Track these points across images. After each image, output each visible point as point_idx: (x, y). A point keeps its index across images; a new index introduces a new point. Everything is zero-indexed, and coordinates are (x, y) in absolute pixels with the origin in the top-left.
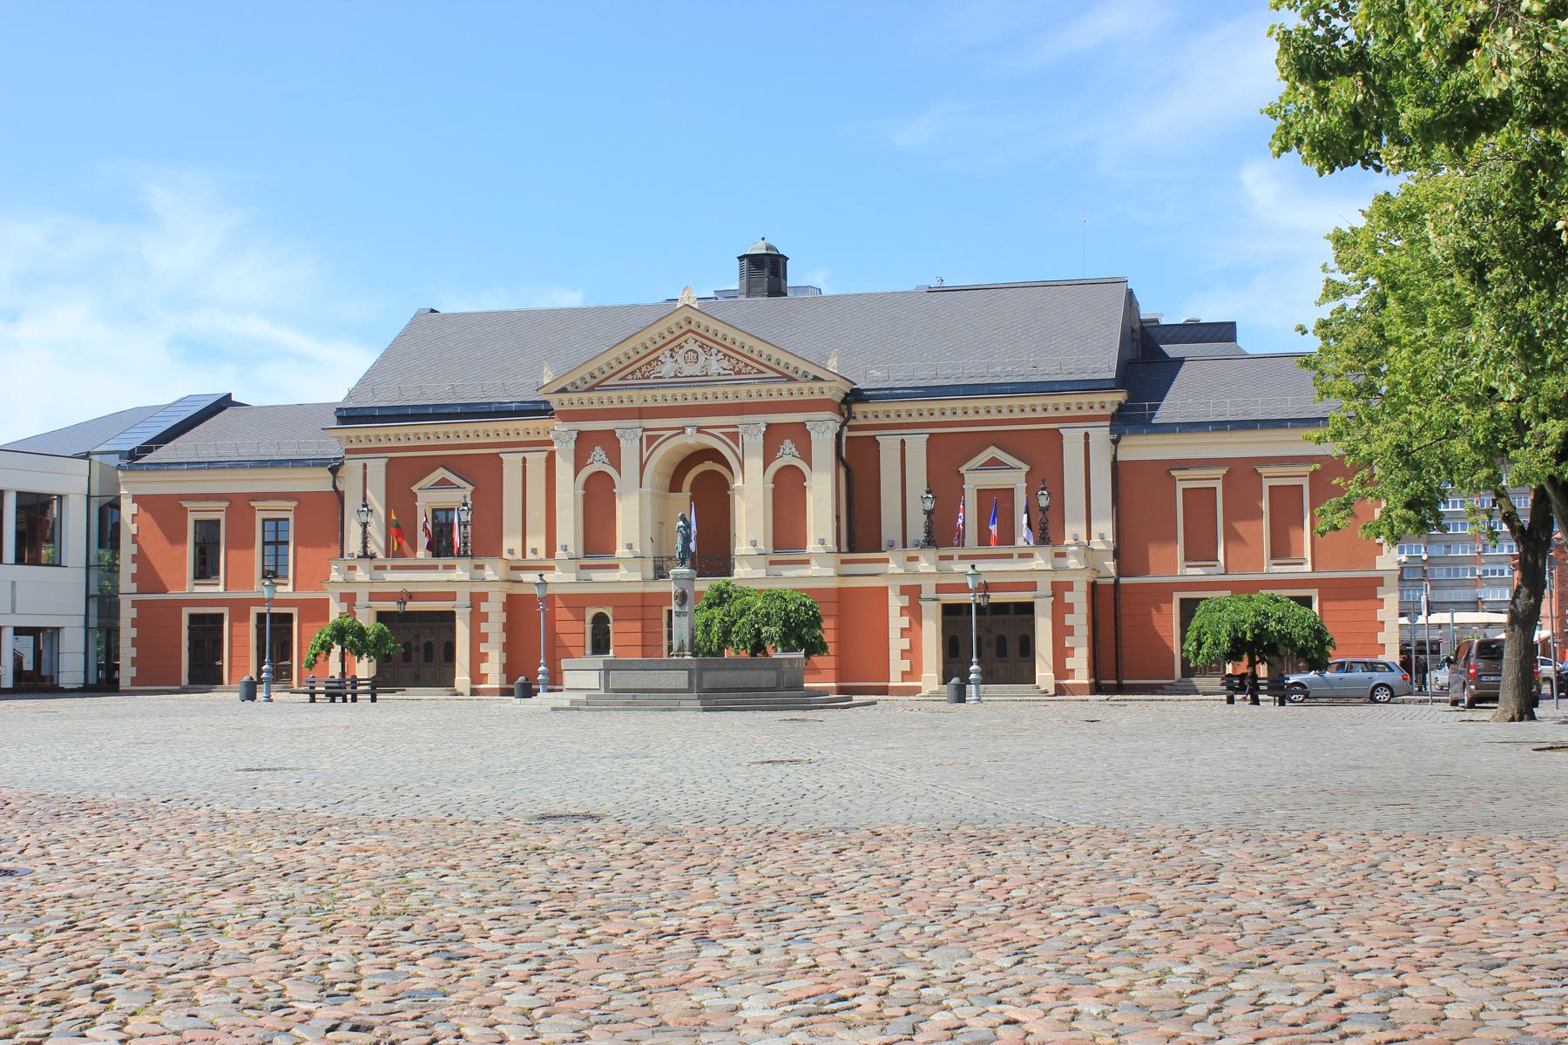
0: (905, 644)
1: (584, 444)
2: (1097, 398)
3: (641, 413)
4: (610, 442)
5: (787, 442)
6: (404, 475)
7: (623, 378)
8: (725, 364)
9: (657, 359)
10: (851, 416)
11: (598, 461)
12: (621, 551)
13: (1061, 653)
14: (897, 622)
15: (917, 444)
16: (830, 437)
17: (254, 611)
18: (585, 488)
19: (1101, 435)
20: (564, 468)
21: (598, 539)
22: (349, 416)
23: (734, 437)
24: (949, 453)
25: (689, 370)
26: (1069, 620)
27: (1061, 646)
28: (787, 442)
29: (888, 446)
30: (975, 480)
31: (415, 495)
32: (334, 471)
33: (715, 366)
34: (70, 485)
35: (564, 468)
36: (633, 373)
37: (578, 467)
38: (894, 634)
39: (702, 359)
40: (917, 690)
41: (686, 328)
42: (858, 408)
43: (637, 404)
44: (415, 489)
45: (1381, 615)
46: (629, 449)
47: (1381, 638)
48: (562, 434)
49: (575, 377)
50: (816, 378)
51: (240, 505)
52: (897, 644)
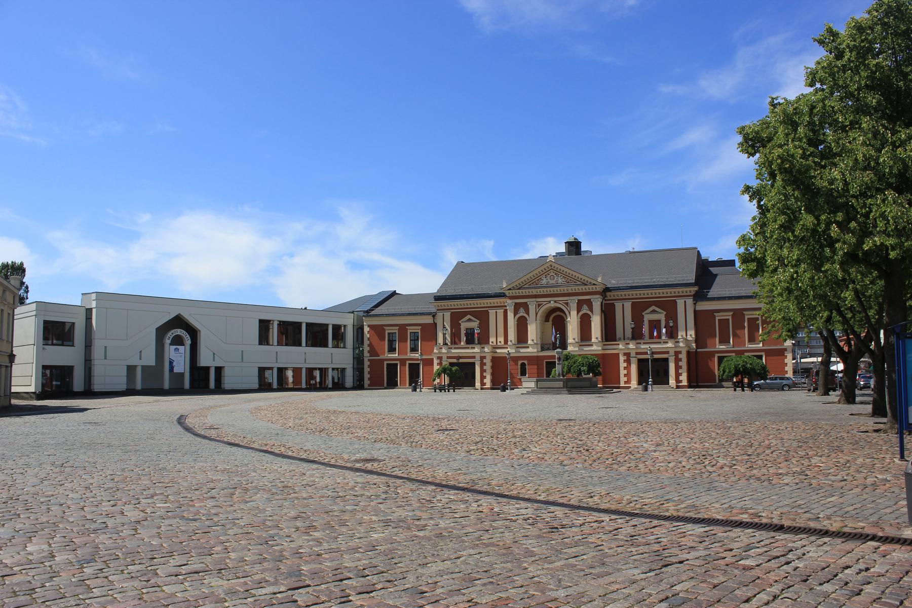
0: (625, 372)
1: (517, 308)
2: (688, 289)
3: (536, 296)
4: (526, 307)
6: (456, 317)
10: (606, 296)
11: (522, 313)
12: (530, 342)
13: (678, 375)
14: (623, 365)
15: (628, 305)
16: (599, 303)
17: (408, 362)
19: (690, 301)
20: (510, 315)
21: (522, 338)
22: (438, 298)
23: (567, 304)
24: (639, 309)
25: (551, 282)
26: (680, 364)
27: (678, 374)
29: (618, 306)
30: (648, 317)
32: (434, 316)
33: (560, 280)
34: (348, 321)
35: (510, 315)
38: (622, 369)
40: (629, 387)
42: (608, 294)
43: (535, 293)
45: (786, 361)
46: (532, 308)
47: (786, 369)
48: (510, 304)
49: (514, 285)
51: (403, 328)
52: (623, 372)
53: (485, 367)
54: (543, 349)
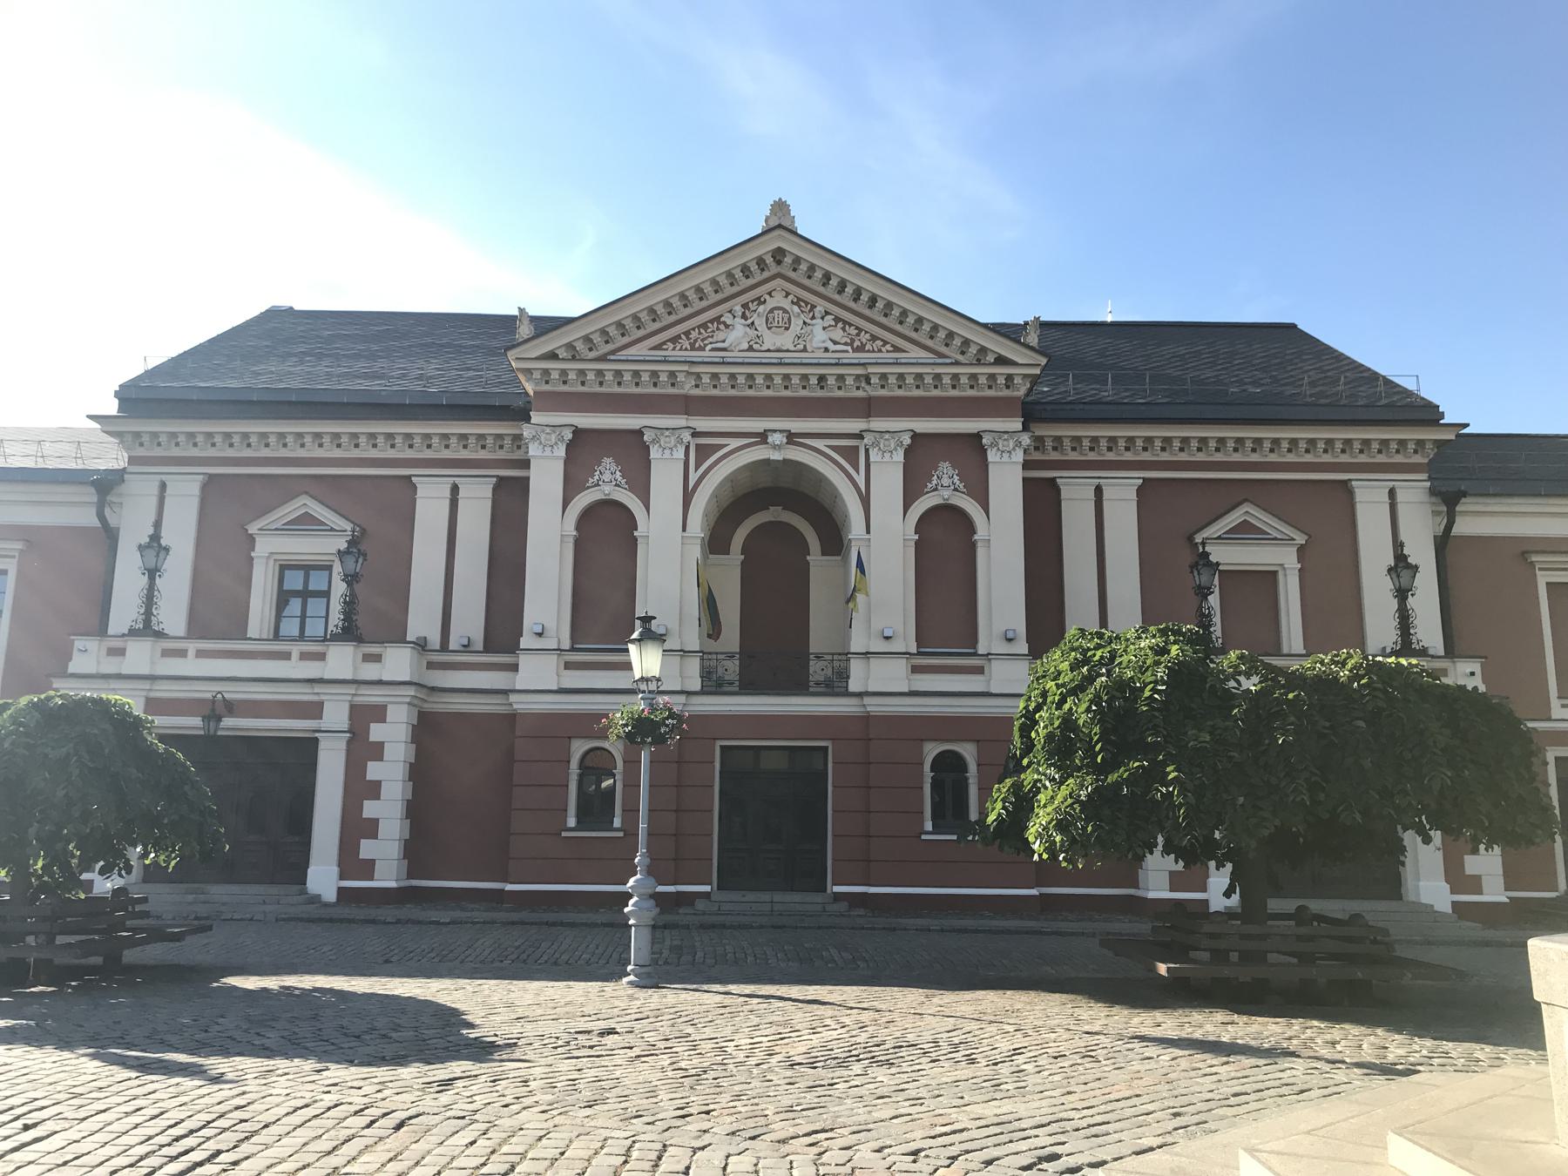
3: (688, 405)
4: (633, 453)
5: (945, 468)
7: (658, 347)
8: (838, 334)
9: (718, 319)
11: (608, 483)
18: (577, 528)
19: (1414, 493)
21: (604, 615)
25: (771, 340)
28: (945, 468)
31: (251, 539)
36: (675, 340)
37: (572, 486)
39: (796, 326)
41: (774, 269)
44: (253, 529)
50: (1001, 361)
53: (374, 771)
54: (713, 683)
